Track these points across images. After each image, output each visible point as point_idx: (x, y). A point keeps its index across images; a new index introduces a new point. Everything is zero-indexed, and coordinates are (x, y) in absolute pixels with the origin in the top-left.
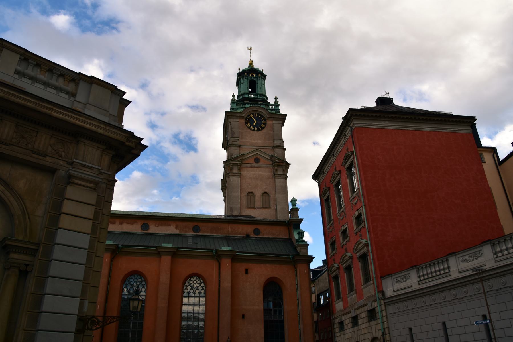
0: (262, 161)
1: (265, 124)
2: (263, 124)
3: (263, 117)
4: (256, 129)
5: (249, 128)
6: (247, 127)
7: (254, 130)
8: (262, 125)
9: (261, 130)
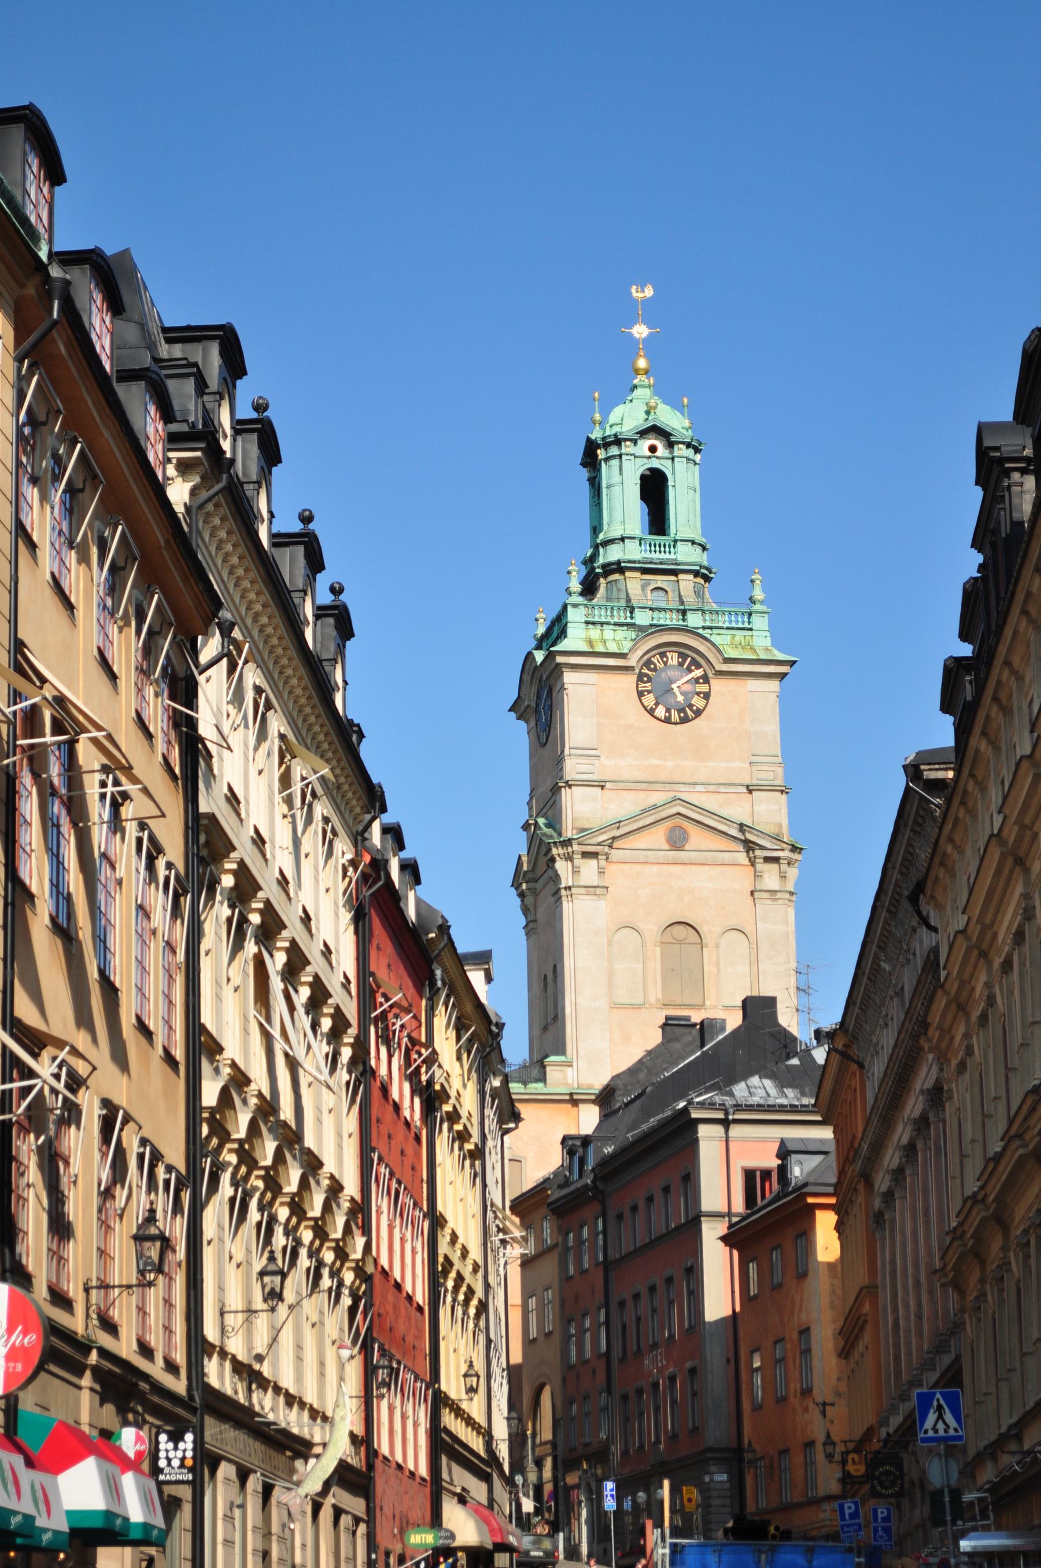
0: (697, 838)
1: (707, 696)
2: (698, 694)
4: (675, 716)
5: (651, 712)
7: (667, 720)
8: (698, 702)
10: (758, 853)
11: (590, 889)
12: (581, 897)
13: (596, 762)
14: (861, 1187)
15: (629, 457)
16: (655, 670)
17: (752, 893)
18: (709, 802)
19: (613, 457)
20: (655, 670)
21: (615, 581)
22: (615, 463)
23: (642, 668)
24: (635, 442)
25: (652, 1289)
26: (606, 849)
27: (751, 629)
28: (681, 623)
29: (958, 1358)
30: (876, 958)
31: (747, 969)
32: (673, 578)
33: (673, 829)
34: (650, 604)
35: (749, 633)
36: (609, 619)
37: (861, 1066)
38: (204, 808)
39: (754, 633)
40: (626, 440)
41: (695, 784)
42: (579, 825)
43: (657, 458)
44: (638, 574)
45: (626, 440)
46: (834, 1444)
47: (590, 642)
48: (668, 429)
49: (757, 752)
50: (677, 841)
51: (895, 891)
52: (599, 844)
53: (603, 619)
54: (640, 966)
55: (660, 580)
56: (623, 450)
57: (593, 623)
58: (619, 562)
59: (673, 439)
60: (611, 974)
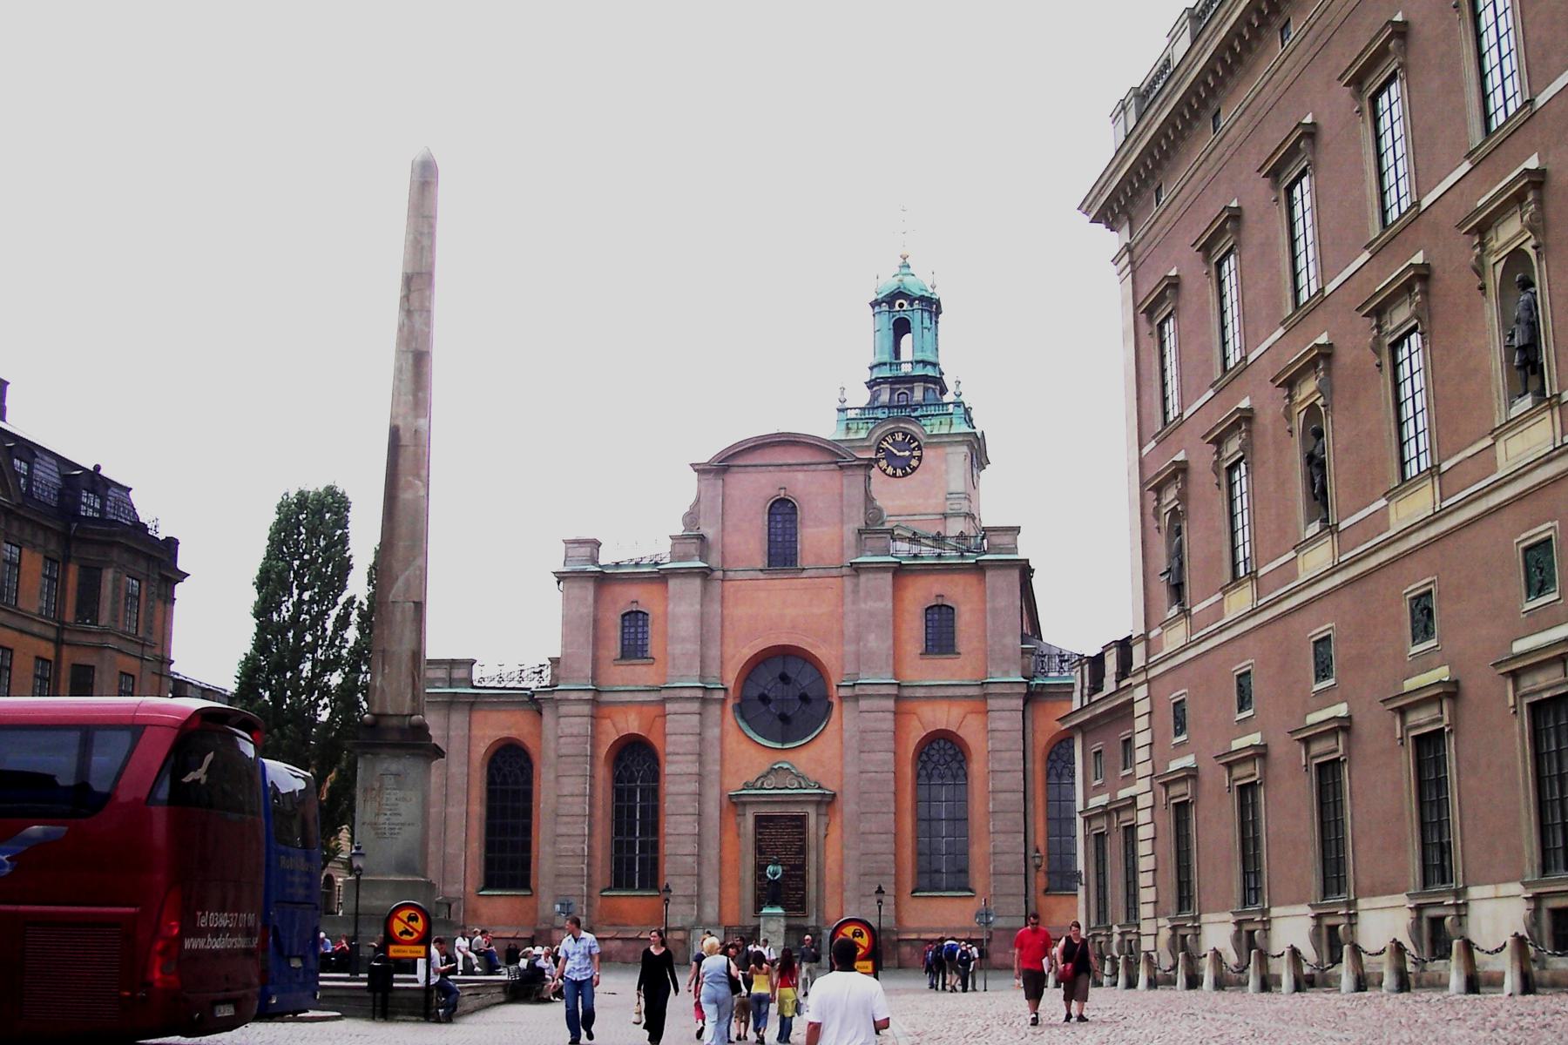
1: (920, 459)
3: (915, 440)
4: (899, 472)
7: (894, 475)
8: (914, 463)
49: (951, 491)
55: (902, 388)
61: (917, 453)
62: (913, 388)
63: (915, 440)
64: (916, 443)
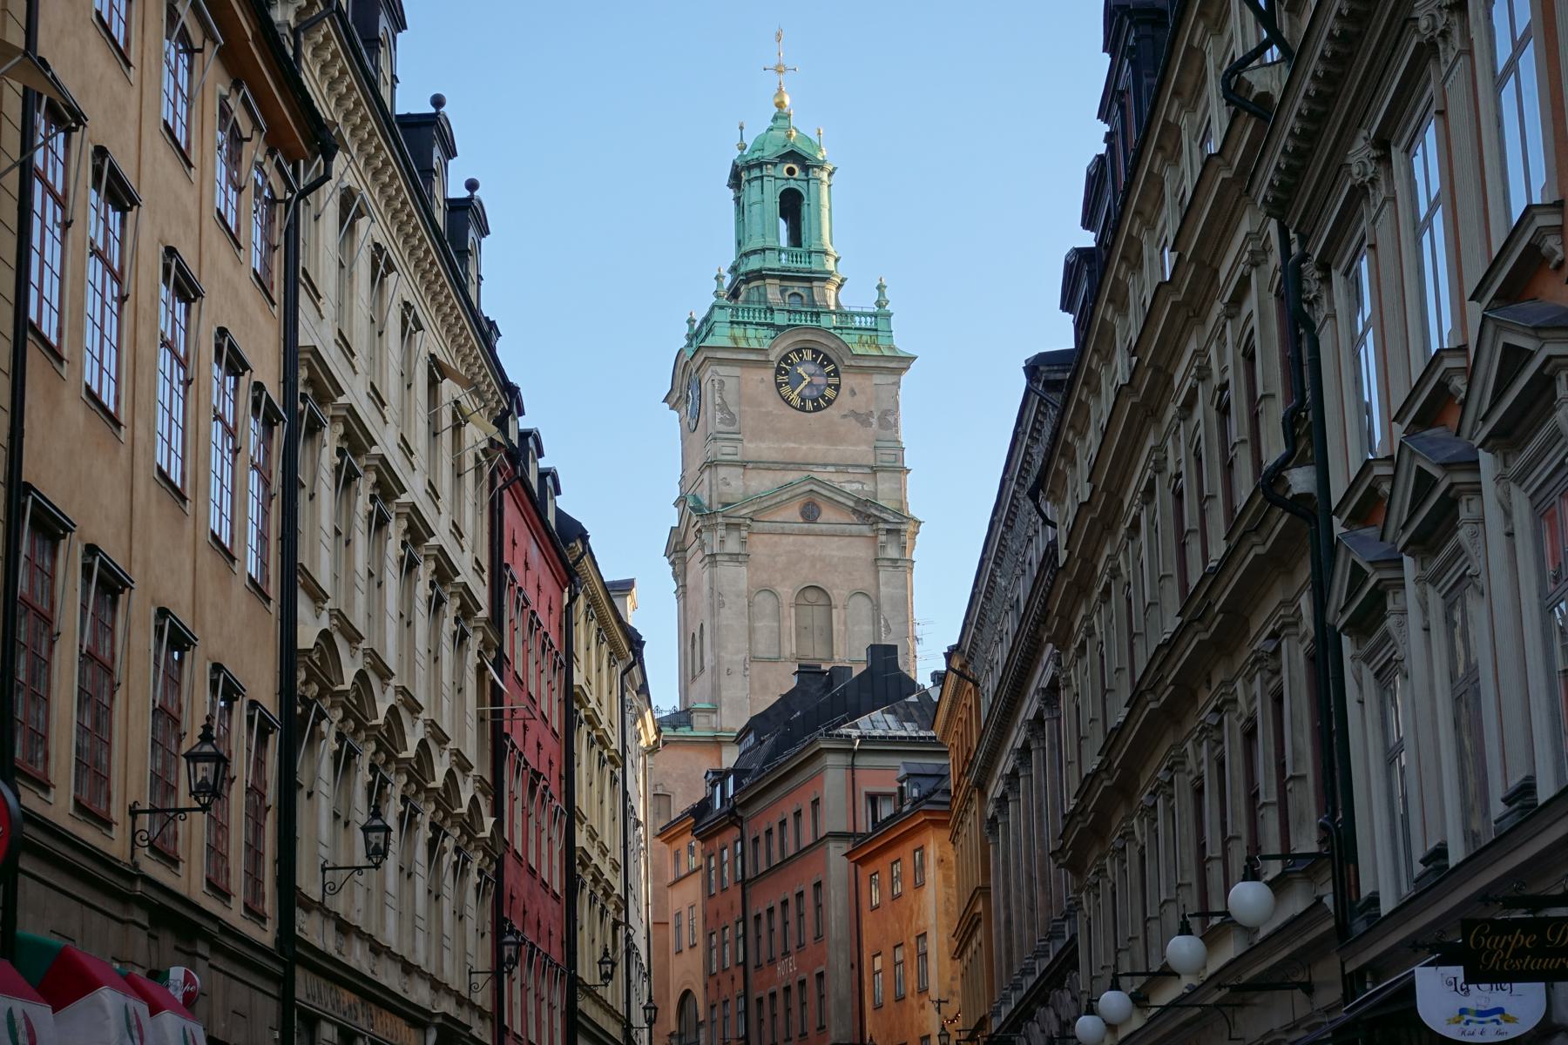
0: (827, 514)
1: (837, 388)
2: (830, 386)
3: (830, 362)
4: (809, 405)
6: (783, 398)
7: (803, 409)
8: (829, 393)
9: (825, 408)
10: (881, 526)
11: (734, 557)
12: (726, 564)
13: (739, 445)
14: (976, 796)
15: (769, 179)
16: (792, 364)
17: (876, 560)
18: (837, 479)
19: (756, 178)
20: (792, 364)
21: (758, 287)
22: (756, 183)
23: (780, 363)
24: (775, 165)
25: (785, 903)
26: (748, 522)
27: (876, 330)
28: (815, 323)
29: (1073, 937)
30: (992, 574)
31: (871, 628)
32: (807, 285)
33: (807, 505)
34: (787, 307)
35: (875, 333)
36: (751, 320)
37: (976, 684)
38: (304, 340)
39: (880, 334)
40: (767, 163)
41: (826, 465)
42: (723, 500)
43: (795, 179)
44: (777, 281)
45: (767, 163)
46: (948, 1035)
47: (734, 339)
48: (804, 154)
50: (810, 513)
51: (1011, 504)
52: (740, 517)
53: (746, 320)
54: (776, 624)
55: (797, 287)
56: (764, 173)
57: (738, 323)
58: (760, 271)
59: (808, 163)
60: (751, 631)
61: (832, 380)
62: (811, 288)
63: (830, 362)
64: (831, 367)
